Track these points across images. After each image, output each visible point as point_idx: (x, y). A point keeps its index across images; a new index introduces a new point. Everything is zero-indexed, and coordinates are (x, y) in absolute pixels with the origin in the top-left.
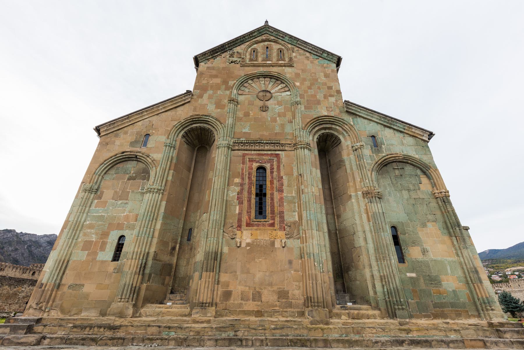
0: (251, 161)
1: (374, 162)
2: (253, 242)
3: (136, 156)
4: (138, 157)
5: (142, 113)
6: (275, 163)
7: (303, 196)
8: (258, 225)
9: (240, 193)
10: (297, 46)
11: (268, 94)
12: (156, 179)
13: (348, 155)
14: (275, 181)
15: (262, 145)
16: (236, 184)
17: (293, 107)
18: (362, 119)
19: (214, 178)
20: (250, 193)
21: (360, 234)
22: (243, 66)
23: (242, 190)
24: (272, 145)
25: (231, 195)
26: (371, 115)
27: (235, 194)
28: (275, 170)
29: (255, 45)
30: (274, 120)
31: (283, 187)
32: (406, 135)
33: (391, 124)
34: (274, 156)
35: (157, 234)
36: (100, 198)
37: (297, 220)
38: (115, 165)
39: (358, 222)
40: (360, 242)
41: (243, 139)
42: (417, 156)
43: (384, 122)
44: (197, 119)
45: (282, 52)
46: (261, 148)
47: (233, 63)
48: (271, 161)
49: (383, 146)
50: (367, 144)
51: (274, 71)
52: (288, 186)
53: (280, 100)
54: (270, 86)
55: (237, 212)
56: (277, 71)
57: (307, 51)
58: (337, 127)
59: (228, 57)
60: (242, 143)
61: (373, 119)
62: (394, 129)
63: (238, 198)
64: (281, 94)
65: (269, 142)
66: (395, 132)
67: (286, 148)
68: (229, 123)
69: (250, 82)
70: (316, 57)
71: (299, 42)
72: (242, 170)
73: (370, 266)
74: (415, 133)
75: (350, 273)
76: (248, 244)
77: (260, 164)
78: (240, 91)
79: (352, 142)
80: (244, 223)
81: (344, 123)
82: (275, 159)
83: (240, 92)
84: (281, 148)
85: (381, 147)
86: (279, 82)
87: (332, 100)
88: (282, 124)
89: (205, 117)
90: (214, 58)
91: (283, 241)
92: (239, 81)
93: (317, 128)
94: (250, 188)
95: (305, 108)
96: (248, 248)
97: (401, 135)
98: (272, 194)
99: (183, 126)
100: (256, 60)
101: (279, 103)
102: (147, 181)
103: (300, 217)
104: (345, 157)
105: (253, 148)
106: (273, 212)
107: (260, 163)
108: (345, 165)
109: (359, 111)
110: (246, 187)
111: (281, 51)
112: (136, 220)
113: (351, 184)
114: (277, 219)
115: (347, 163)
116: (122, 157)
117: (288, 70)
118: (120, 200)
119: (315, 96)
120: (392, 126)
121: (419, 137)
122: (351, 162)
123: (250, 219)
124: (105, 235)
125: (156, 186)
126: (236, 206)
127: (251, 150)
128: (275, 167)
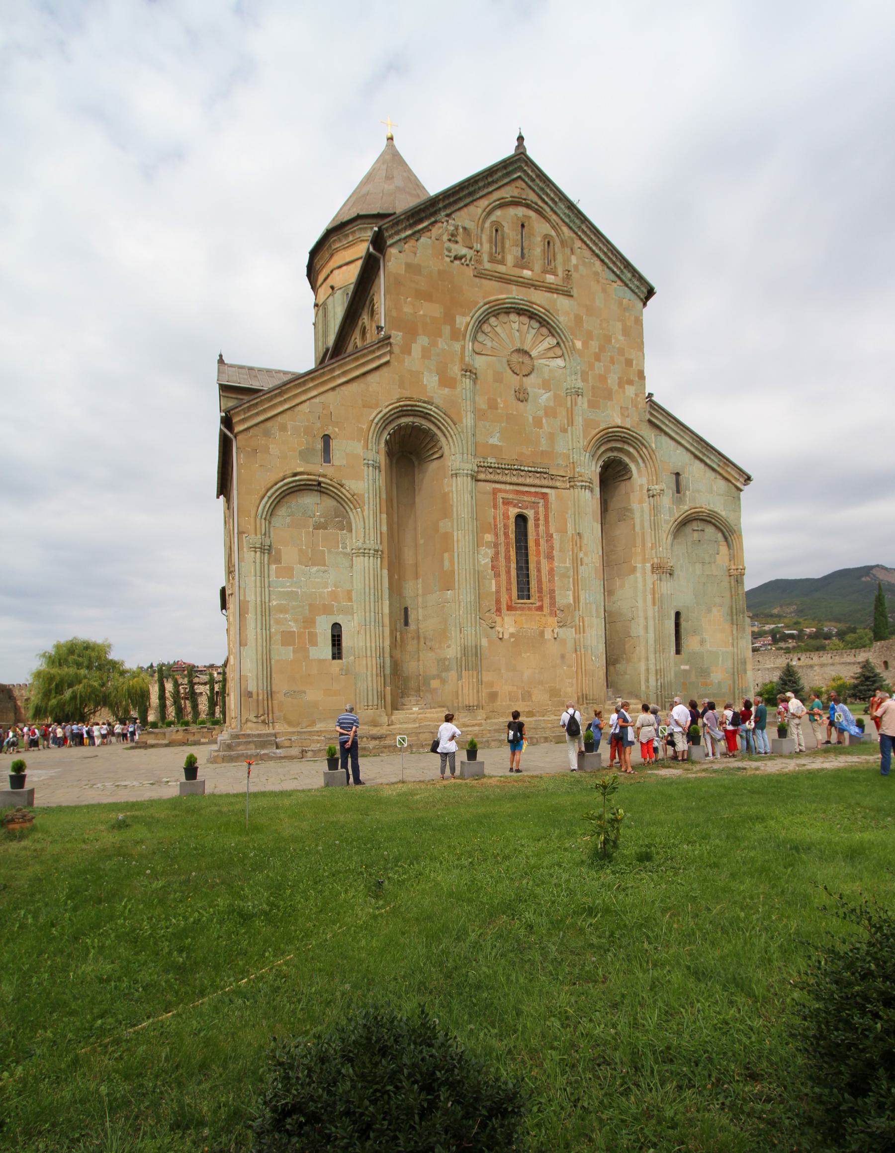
0: (506, 502)
1: (673, 519)
2: (518, 632)
3: (319, 484)
4: (323, 485)
5: (304, 383)
6: (541, 510)
7: (581, 569)
8: (522, 609)
9: (495, 558)
10: (579, 236)
11: (526, 360)
12: (367, 531)
13: (641, 502)
14: (542, 542)
15: (522, 473)
16: (488, 545)
17: (569, 397)
18: (668, 439)
19: (455, 534)
20: (508, 559)
21: (642, 621)
22: (480, 275)
23: (497, 554)
24: (538, 475)
25: (483, 562)
26: (682, 434)
27: (488, 560)
28: (541, 522)
29: (498, 213)
30: (538, 423)
31: (552, 552)
32: (718, 477)
33: (704, 455)
34: (541, 496)
35: (387, 621)
36: (278, 561)
37: (572, 602)
38: (284, 497)
39: (640, 604)
40: (637, 630)
41: (493, 461)
42: (723, 513)
43: (697, 449)
44: (409, 408)
45: (551, 244)
46: (520, 480)
48: (534, 505)
49: (687, 493)
50: (668, 488)
51: (538, 302)
52: (560, 551)
53: (547, 377)
54: (530, 337)
55: (494, 589)
56: (544, 303)
57: (598, 256)
58: (631, 450)
60: (490, 467)
61: (683, 442)
62: (706, 464)
63: (493, 568)
64: (547, 363)
65: (533, 469)
66: (707, 469)
67: (558, 484)
68: (469, 425)
69: (493, 320)
70: (613, 277)
71: (584, 227)
72: (495, 518)
73: (647, 659)
74: (729, 473)
75: (618, 666)
76: (512, 635)
77: (519, 510)
78: (476, 343)
79: (648, 480)
80: (504, 607)
81: (643, 444)
82: (542, 501)
83: (478, 347)
84: (551, 483)
85: (684, 494)
86: (544, 331)
87: (630, 391)
88: (550, 433)
89: (425, 405)
91: (556, 631)
93: (603, 449)
94: (507, 551)
95: (589, 406)
96: (512, 640)
97: (712, 475)
98: (538, 563)
99: (387, 421)
100: (502, 262)
101: (546, 385)
102: (348, 534)
103: (577, 599)
104: (635, 506)
105: (508, 479)
106: (540, 590)
107: (520, 508)
108: (633, 519)
109: (667, 423)
110: (502, 549)
111: (549, 243)
112: (350, 600)
113: (639, 550)
114: (547, 601)
115: (637, 516)
116: (294, 484)
117: (562, 302)
118: (314, 565)
119: (603, 378)
120: (705, 458)
121: (733, 481)
122: (642, 516)
123: (511, 600)
124: (309, 622)
125: (371, 544)
126: (491, 579)
127: (505, 483)
128: (542, 517)
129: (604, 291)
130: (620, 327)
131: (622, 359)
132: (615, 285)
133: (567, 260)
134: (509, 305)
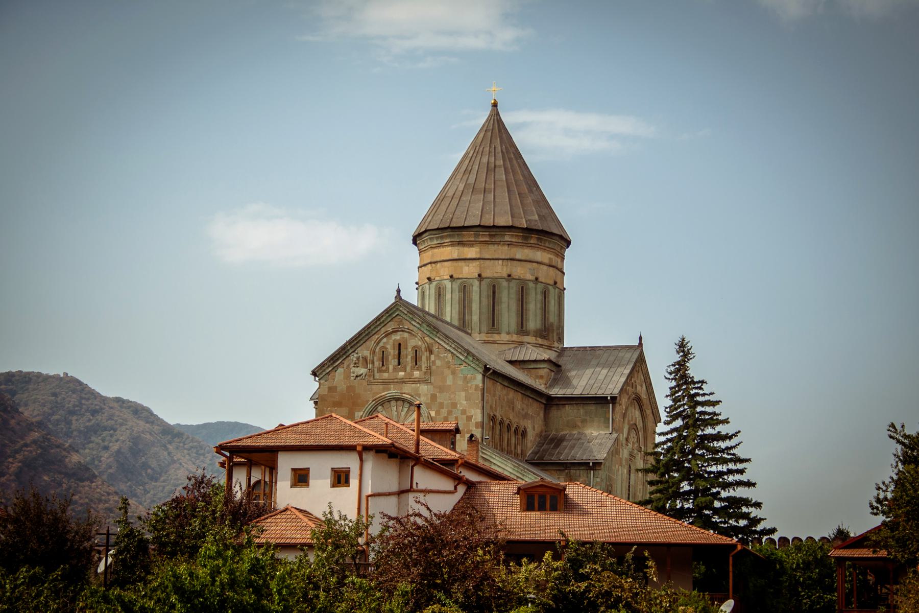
22: (370, 383)
26: (505, 463)
43: (518, 472)
47: (359, 378)
59: (352, 365)
90: (335, 369)
92: (365, 412)
109: (494, 457)
117: (424, 388)
129: (453, 373)
130: (464, 395)
131: (464, 417)
132: (462, 367)
133: (428, 359)
134: (389, 398)
